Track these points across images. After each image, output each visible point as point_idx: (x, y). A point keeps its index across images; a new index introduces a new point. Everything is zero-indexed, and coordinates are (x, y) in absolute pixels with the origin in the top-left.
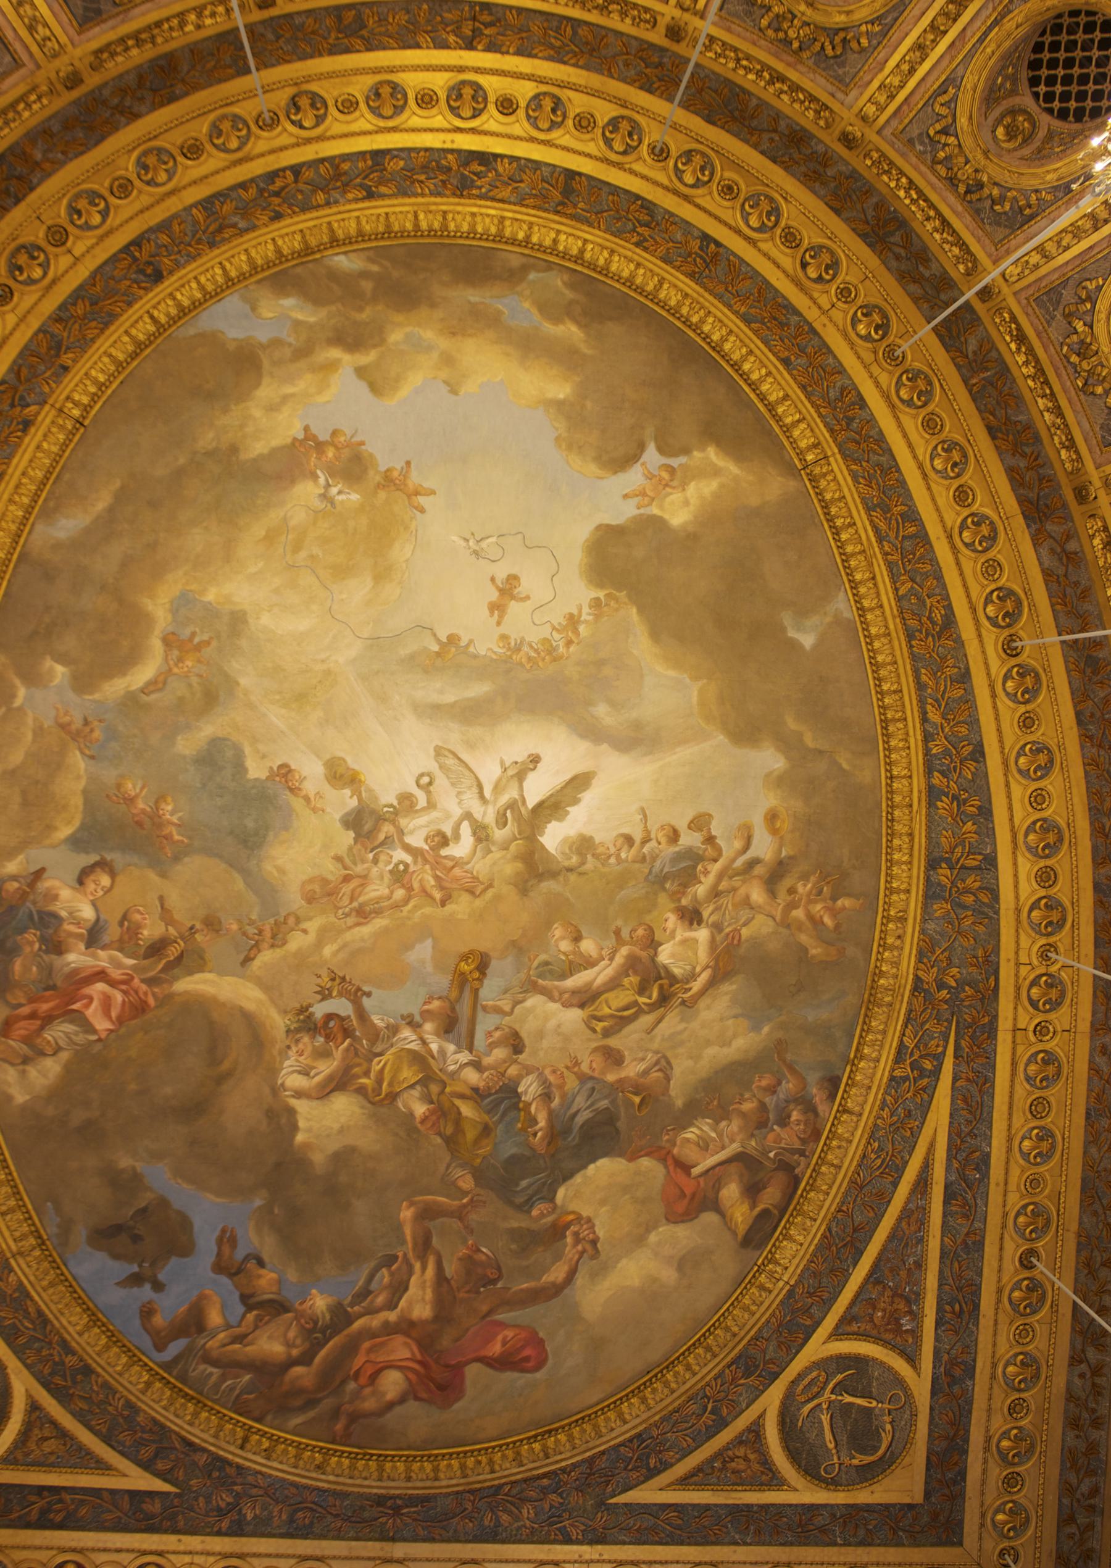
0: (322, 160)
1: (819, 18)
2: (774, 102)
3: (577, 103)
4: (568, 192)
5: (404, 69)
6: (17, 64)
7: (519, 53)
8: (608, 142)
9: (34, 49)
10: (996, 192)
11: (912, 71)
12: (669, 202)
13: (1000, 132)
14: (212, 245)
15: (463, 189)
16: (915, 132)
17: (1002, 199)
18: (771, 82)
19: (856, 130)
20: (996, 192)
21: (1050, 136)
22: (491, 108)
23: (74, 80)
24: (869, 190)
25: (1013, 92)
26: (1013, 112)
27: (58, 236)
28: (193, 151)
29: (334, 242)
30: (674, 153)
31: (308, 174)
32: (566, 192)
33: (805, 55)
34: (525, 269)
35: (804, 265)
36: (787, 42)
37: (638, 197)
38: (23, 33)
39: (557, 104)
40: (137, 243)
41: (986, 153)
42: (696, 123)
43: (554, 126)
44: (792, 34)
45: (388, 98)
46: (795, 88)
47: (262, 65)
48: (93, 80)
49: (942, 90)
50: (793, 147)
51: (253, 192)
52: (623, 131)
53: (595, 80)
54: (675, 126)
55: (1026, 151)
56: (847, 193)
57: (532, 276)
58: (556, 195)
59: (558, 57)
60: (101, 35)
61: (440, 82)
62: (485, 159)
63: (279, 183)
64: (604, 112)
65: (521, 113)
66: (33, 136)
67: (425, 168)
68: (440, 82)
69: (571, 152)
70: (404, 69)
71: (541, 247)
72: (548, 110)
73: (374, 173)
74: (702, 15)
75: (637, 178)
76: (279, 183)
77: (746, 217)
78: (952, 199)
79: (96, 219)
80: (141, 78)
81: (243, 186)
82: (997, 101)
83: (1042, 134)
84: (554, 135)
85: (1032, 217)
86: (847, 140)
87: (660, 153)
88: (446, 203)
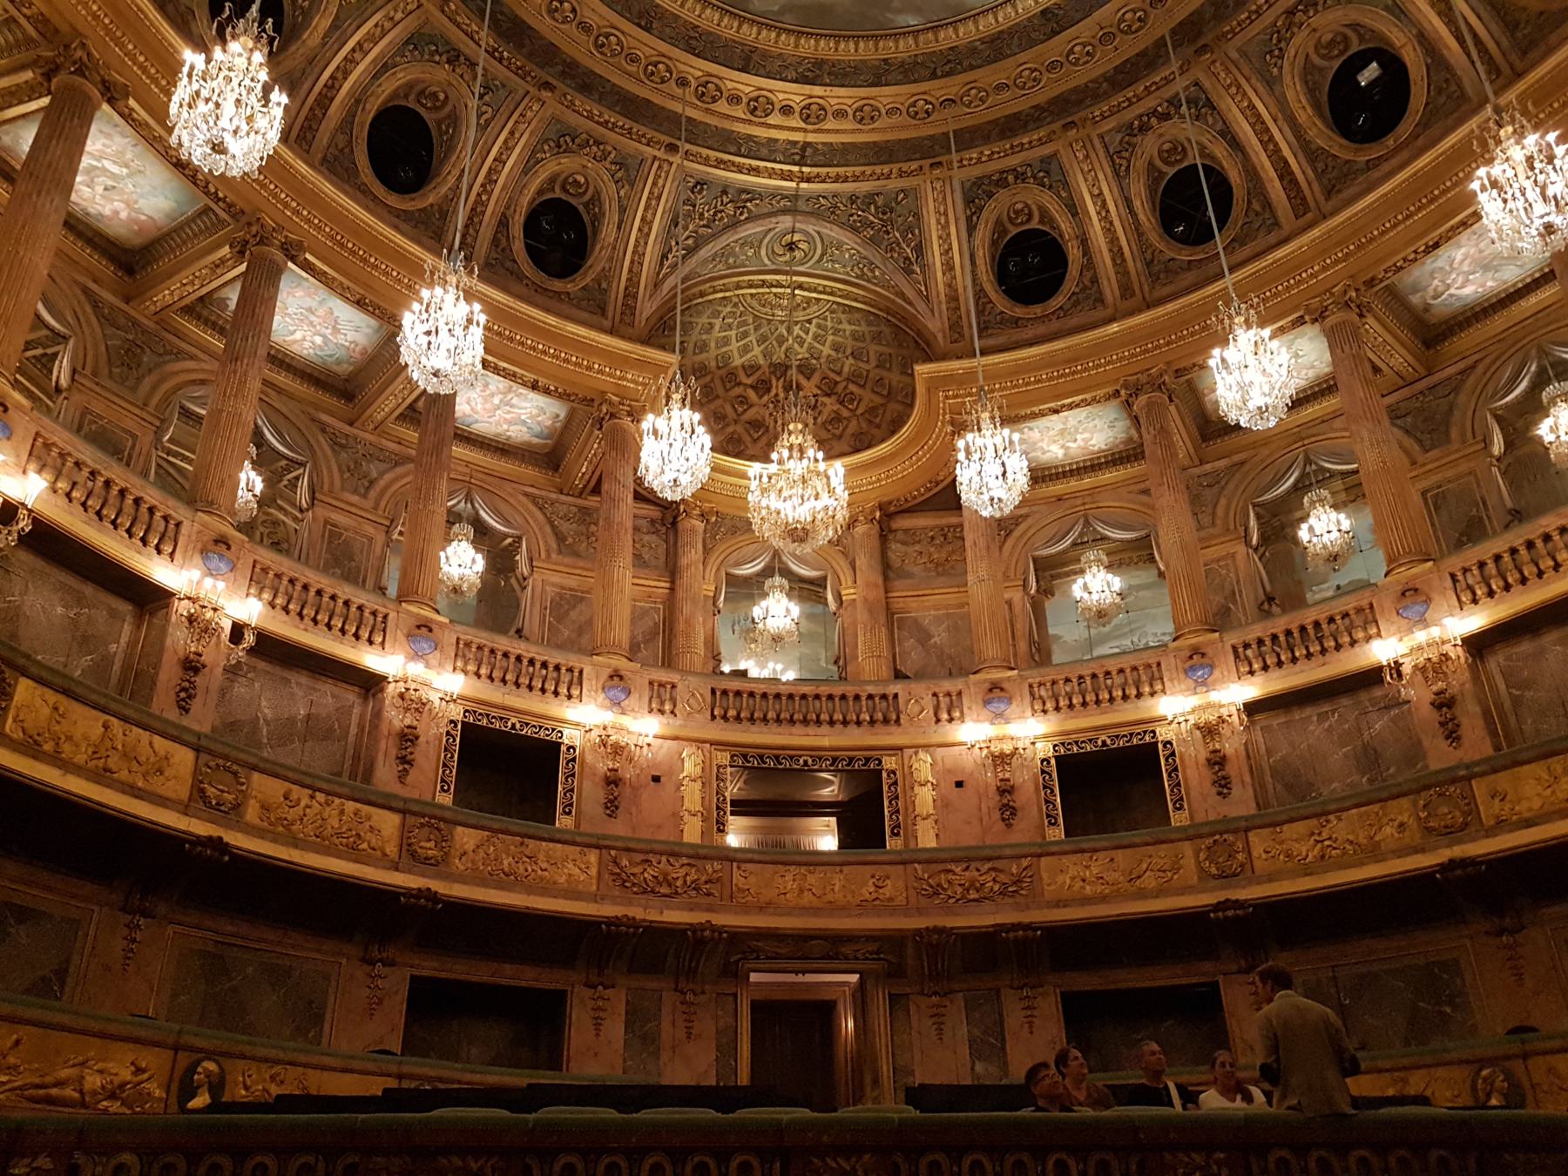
0: (915, 81)
1: (577, 159)
2: (603, 109)
3: (739, 111)
4: (748, 59)
5: (853, 131)
6: (1101, 137)
7: (777, 140)
8: (718, 89)
9: (1089, 146)
10: (437, 58)
11: (512, 133)
12: (676, 53)
13: (442, 96)
14: (1001, 32)
15: (819, 63)
16: (502, 93)
17: (432, 54)
18: (607, 122)
19: (546, 94)
20: (437, 58)
21: (406, 96)
22: (797, 109)
23: (1066, 127)
24: (530, 56)
25: (439, 122)
26: (436, 109)
27: (1107, 38)
28: (1001, 88)
29: (916, 33)
30: (673, 82)
31: (927, 73)
32: (748, 61)
33: (584, 136)
34: (782, 11)
35: (574, 10)
36: (597, 143)
37: (698, 56)
38: (1093, 155)
39: (753, 111)
40: (1055, 33)
41: (450, 84)
42: (657, 99)
43: (756, 99)
44: (595, 148)
45: (864, 115)
46: (590, 118)
47: (946, 134)
48: (1057, 126)
49: (488, 123)
50: (588, 84)
51: (965, 64)
52: (707, 92)
53: (727, 125)
54: (673, 97)
55: (420, 87)
56: (546, 54)
57: (776, 8)
58: (755, 57)
59: (750, 137)
60: (1046, 150)
61: (830, 124)
62: (802, 80)
63: (947, 68)
64: (722, 106)
65: (778, 106)
66: (1107, 95)
67: (846, 75)
68: (830, 124)
69: (746, 84)
70: (853, 131)
71: (770, 27)
72: (759, 107)
73: (879, 75)
74: (655, 158)
75: (696, 68)
76: (947, 68)
77: (619, 42)
78: (467, 51)
79: (1077, 49)
80: (1025, 126)
81: (972, 68)
82: (449, 116)
83: (412, 97)
84: (756, 94)
85: (407, 42)
86: (547, 86)
87: (682, 82)
88: (831, 56)
